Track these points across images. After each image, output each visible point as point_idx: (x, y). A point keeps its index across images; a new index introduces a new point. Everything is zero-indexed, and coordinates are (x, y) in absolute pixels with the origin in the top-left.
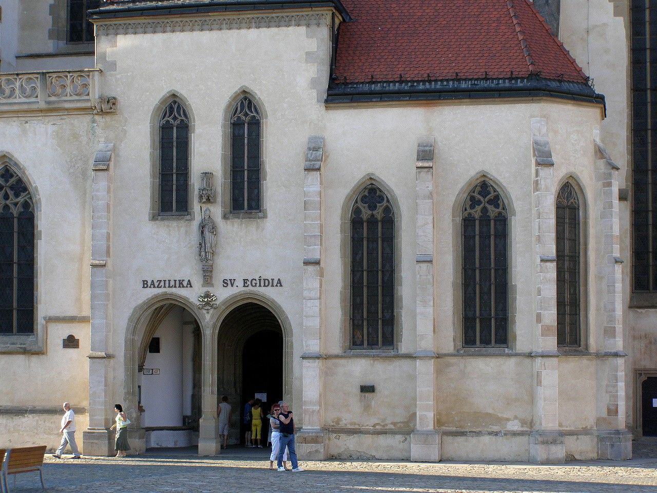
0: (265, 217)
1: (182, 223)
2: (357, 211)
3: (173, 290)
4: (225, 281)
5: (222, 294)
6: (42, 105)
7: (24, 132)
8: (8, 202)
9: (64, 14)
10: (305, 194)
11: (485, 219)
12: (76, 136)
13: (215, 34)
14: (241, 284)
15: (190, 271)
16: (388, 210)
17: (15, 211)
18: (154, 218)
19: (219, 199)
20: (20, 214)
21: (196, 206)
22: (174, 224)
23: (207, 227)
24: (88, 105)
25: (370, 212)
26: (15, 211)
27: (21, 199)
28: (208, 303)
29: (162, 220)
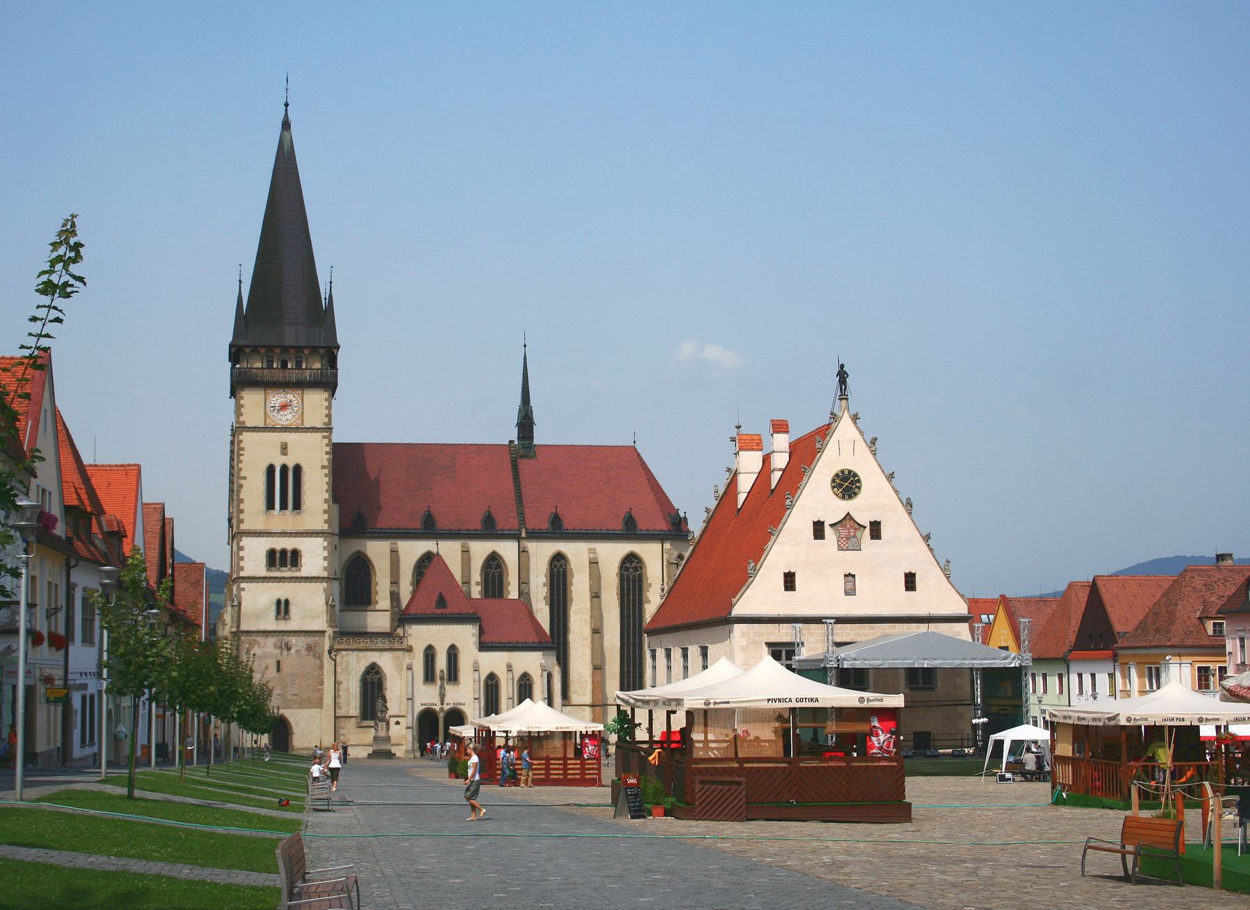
1: (433, 686)
2: (487, 682)
3: (432, 707)
5: (446, 708)
6: (388, 647)
9: (344, 594)
11: (525, 686)
12: (398, 657)
13: (444, 626)
14: (452, 704)
15: (437, 700)
16: (496, 682)
17: (376, 680)
18: (424, 684)
20: (378, 682)
22: (431, 686)
23: (442, 687)
26: (376, 680)
27: (378, 676)
28: (442, 711)
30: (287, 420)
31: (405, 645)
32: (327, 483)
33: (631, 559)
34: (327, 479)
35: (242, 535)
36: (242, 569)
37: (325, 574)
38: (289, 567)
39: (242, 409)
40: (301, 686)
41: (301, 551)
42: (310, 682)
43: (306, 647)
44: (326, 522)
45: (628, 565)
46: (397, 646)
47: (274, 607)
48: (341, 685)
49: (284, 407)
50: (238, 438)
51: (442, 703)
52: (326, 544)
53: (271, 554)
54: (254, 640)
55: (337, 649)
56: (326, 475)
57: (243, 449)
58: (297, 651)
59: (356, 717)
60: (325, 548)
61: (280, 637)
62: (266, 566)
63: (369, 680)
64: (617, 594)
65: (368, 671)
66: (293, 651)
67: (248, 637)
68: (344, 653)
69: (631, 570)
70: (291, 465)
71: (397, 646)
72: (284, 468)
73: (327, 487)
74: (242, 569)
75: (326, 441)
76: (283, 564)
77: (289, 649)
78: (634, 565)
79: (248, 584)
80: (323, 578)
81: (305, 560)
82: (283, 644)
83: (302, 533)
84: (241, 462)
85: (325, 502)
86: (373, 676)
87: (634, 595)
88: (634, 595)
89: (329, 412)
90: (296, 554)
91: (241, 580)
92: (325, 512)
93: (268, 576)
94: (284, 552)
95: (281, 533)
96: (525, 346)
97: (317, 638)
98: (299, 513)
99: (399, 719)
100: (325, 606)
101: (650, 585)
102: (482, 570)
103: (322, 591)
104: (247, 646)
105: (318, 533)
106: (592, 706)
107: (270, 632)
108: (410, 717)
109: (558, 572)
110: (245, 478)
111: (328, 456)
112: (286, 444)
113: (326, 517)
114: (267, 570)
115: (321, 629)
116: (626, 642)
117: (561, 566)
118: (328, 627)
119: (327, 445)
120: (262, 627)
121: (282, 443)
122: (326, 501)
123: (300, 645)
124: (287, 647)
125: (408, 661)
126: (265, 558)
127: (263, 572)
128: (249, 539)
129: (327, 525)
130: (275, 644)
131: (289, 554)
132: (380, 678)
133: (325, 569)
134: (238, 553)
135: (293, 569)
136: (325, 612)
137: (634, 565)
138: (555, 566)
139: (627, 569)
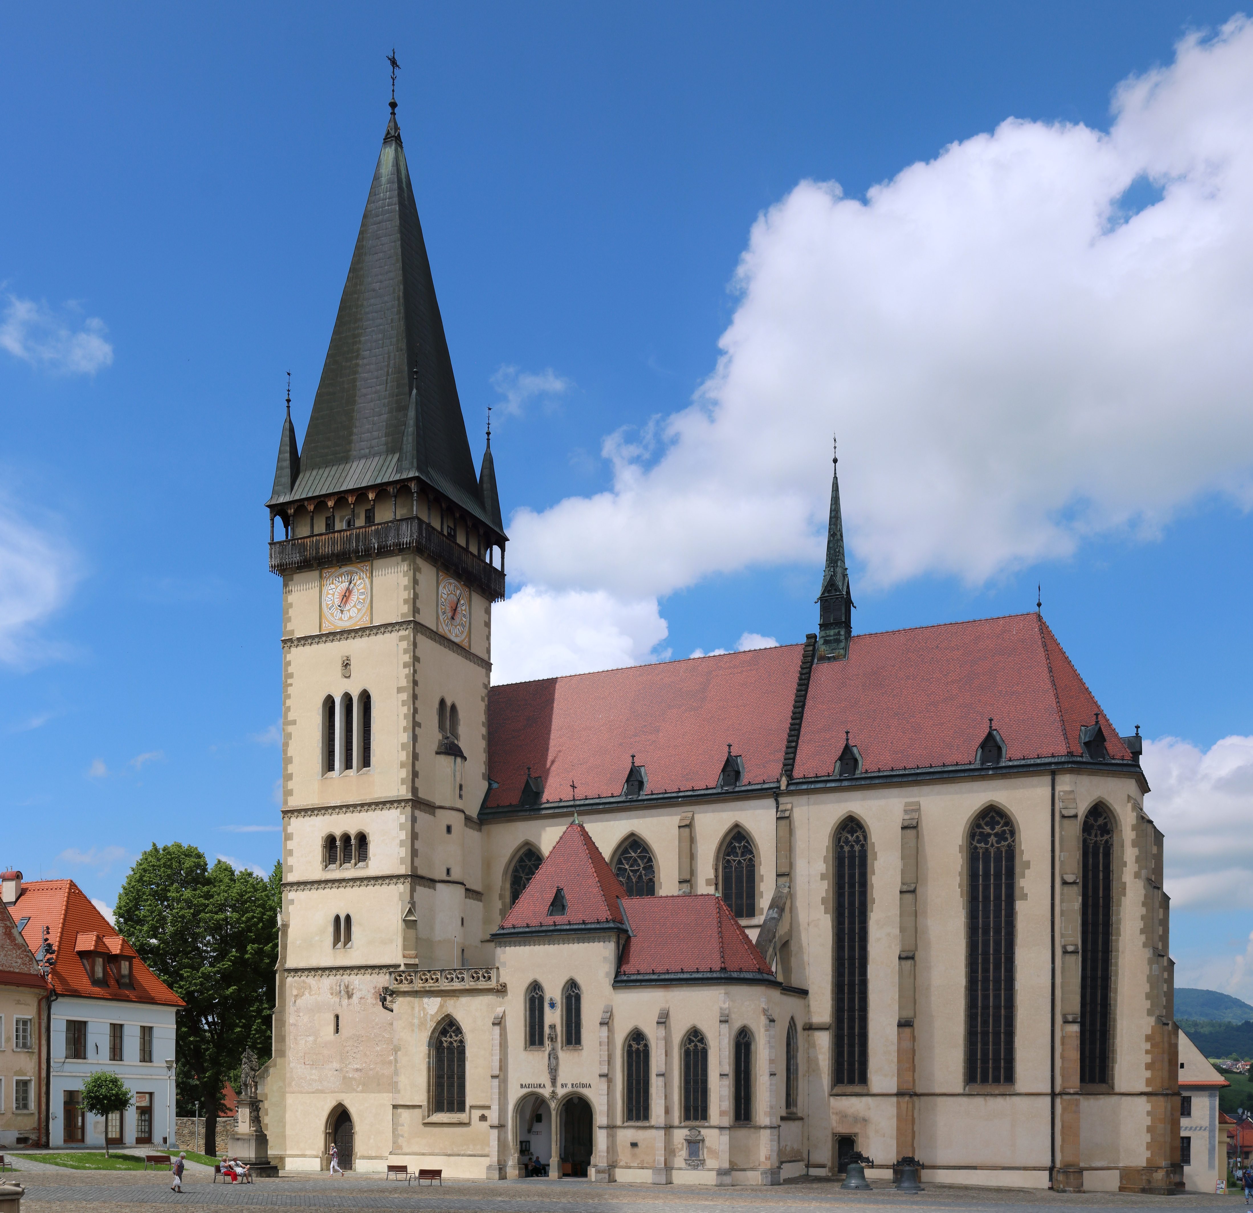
0: (582, 1049)
1: (540, 1053)
4: (562, 1085)
5: (561, 1092)
6: (467, 987)
8: (452, 1040)
10: (600, 1037)
15: (545, 1079)
19: (559, 1039)
20: (458, 1047)
21: (547, 1042)
22: (536, 1053)
23: (553, 1056)
24: (491, 987)
25: (637, 1046)
26: (455, 1044)
29: (530, 1050)
31: (493, 984)
32: (406, 716)
33: (993, 817)
34: (405, 710)
37: (403, 870)
38: (353, 861)
39: (290, 611)
40: (365, 1055)
42: (378, 1048)
44: (403, 782)
45: (987, 830)
46: (482, 984)
48: (399, 1053)
50: (285, 657)
51: (554, 1081)
52: (403, 819)
53: (330, 841)
58: (361, 998)
59: (420, 1107)
60: (402, 827)
61: (338, 977)
63: (445, 1044)
64: (960, 886)
65: (444, 1029)
66: (355, 999)
69: (993, 839)
71: (482, 984)
72: (347, 699)
73: (403, 723)
76: (347, 858)
77: (350, 996)
78: (998, 829)
80: (398, 877)
81: (373, 848)
83: (370, 804)
85: (403, 749)
86: (451, 1037)
87: (998, 887)
88: (998, 887)
90: (362, 839)
94: (346, 838)
95: (341, 807)
98: (369, 770)
99: (486, 1112)
101: (1027, 865)
102: (717, 858)
104: (295, 992)
105: (392, 802)
106: (899, 1094)
107: (324, 969)
108: (495, 1107)
109: (852, 852)
112: (348, 659)
116: (980, 978)
117: (857, 841)
121: (342, 657)
124: (348, 992)
125: (499, 1011)
127: (317, 872)
128: (300, 819)
129: (405, 786)
132: (461, 1042)
134: (286, 846)
135: (361, 864)
137: (998, 829)
138: (847, 842)
139: (984, 838)
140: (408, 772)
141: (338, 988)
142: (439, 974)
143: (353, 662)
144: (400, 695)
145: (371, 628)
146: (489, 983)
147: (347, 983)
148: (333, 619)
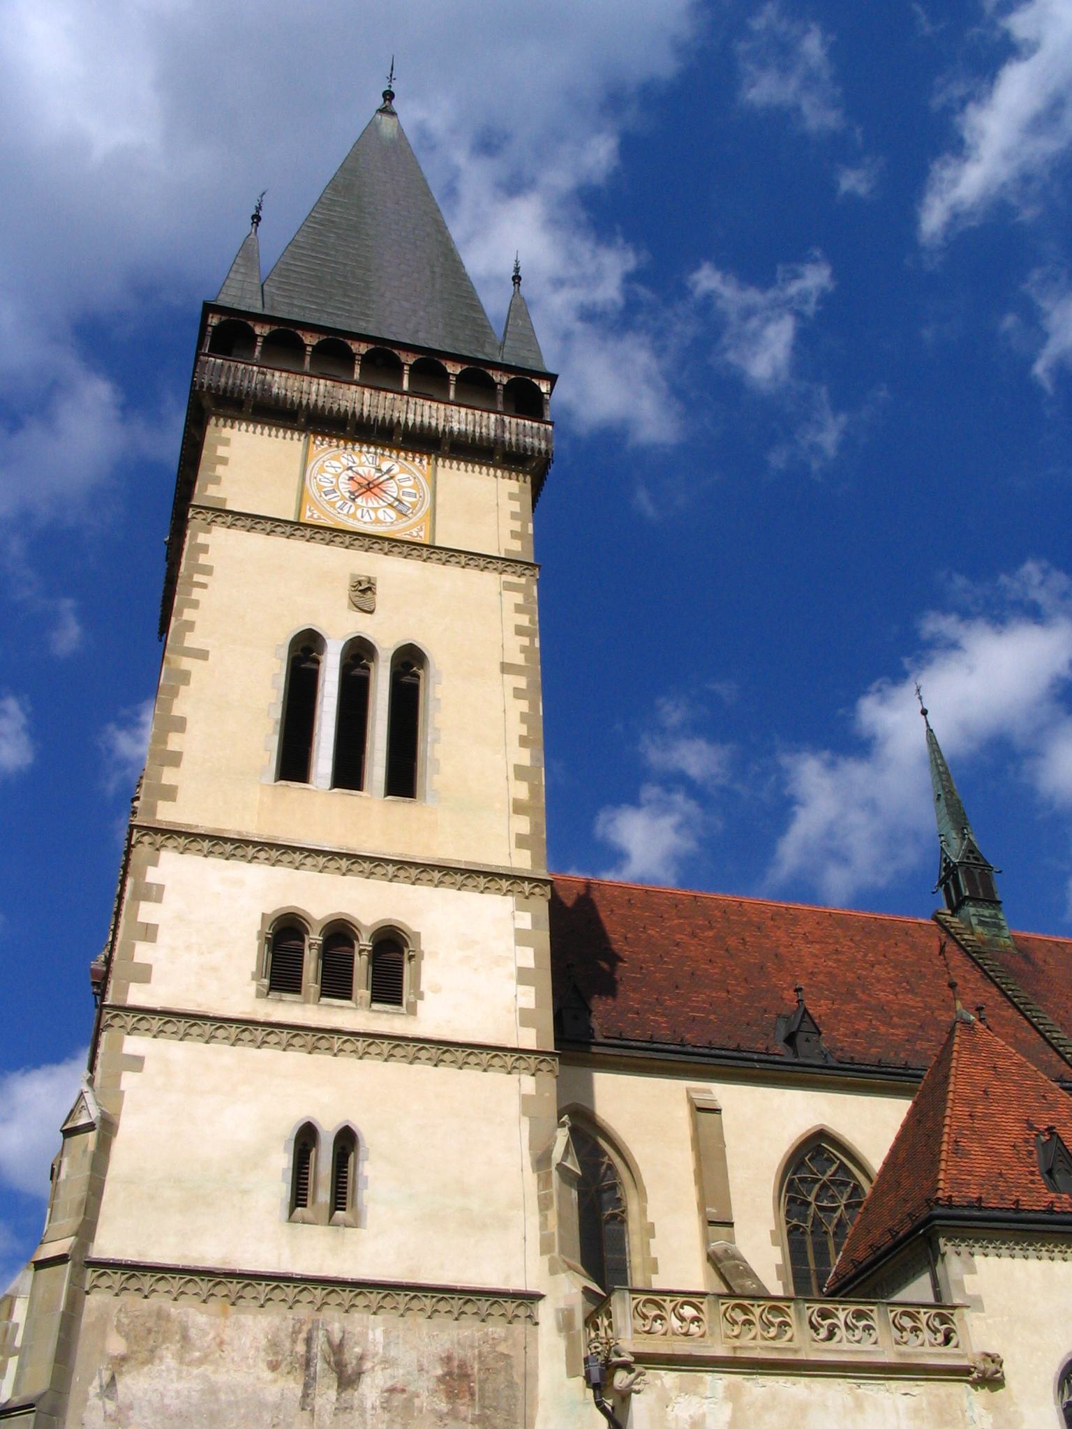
6: (888, 1356)
7: (859, 1405)
24: (965, 1362)
30: (377, 521)
32: (524, 718)
34: (523, 706)
35: (159, 839)
36: (144, 974)
37: (528, 1039)
41: (418, 934)
43: (439, 1372)
44: (521, 841)
47: (283, 1161)
49: (369, 487)
52: (525, 921)
54: (161, 1315)
55: (641, 1358)
56: (518, 694)
57: (208, 570)
58: (392, 1390)
60: (521, 938)
61: (303, 1311)
62: (255, 977)
66: (370, 1389)
67: (128, 1298)
68: (668, 1378)
70: (386, 648)
74: (144, 974)
75: (518, 598)
77: (347, 1379)
79: (160, 1042)
82: (320, 1345)
84: (195, 605)
89: (524, 526)
91: (131, 1020)
92: (518, 808)
93: (261, 1018)
96: (924, 712)
97: (496, 1329)
100: (531, 1178)
103: (514, 1107)
110: (202, 655)
111: (525, 641)
113: (523, 825)
114: (259, 995)
115: (516, 1284)
118: (553, 1271)
119: (519, 609)
120: (210, 1255)
122: (520, 773)
123: (407, 1357)
126: (256, 944)
130: (274, 1345)
131: (364, 941)
133: (526, 1018)
136: (533, 1204)
140: (534, 825)
141: (301, 1348)
142: (791, 1311)
143: (380, 588)
144: (505, 675)
145: (432, 547)
146: (949, 1349)
147: (336, 1338)
148: (331, 510)
